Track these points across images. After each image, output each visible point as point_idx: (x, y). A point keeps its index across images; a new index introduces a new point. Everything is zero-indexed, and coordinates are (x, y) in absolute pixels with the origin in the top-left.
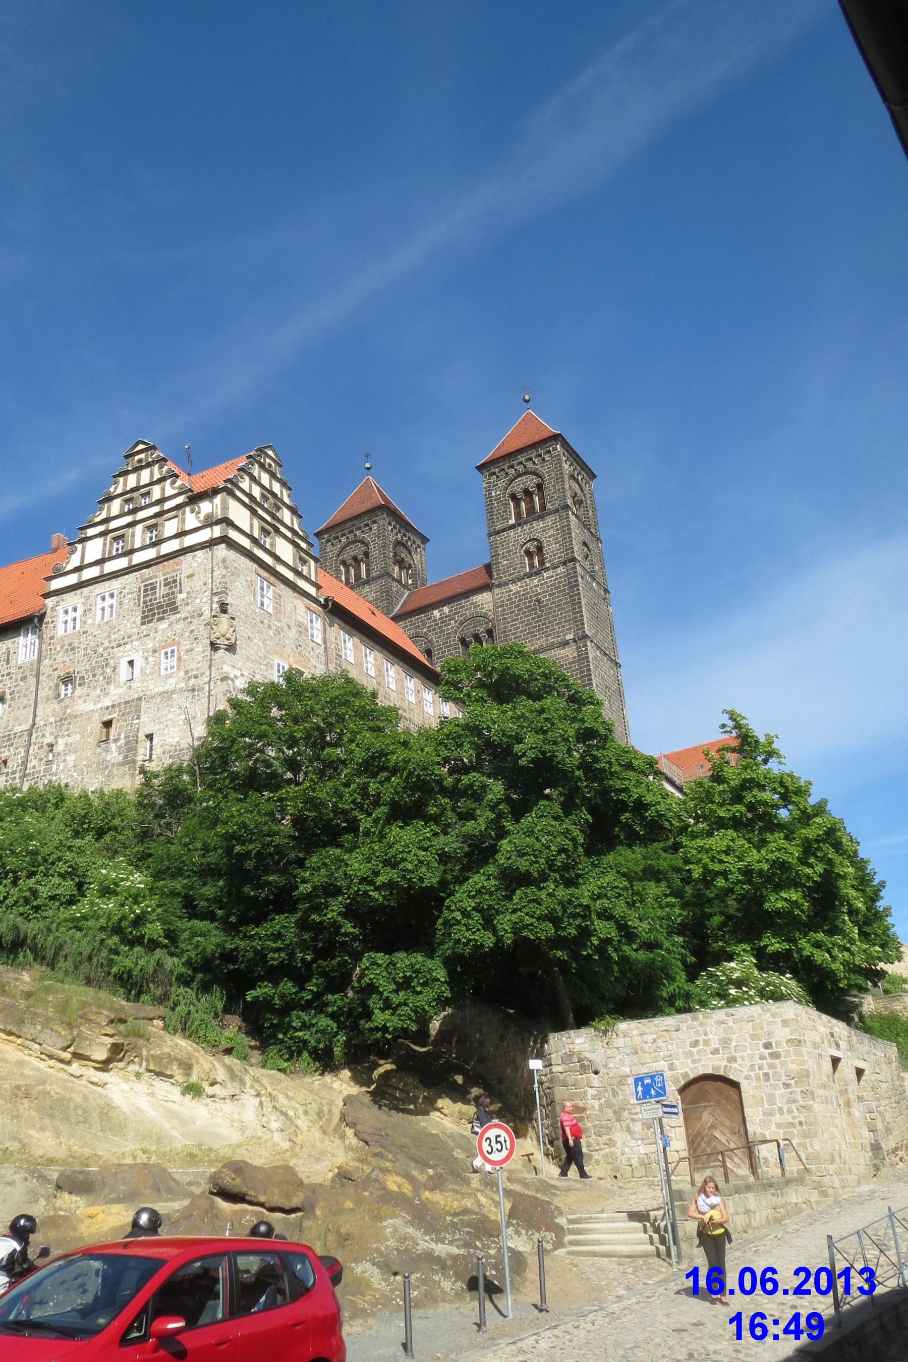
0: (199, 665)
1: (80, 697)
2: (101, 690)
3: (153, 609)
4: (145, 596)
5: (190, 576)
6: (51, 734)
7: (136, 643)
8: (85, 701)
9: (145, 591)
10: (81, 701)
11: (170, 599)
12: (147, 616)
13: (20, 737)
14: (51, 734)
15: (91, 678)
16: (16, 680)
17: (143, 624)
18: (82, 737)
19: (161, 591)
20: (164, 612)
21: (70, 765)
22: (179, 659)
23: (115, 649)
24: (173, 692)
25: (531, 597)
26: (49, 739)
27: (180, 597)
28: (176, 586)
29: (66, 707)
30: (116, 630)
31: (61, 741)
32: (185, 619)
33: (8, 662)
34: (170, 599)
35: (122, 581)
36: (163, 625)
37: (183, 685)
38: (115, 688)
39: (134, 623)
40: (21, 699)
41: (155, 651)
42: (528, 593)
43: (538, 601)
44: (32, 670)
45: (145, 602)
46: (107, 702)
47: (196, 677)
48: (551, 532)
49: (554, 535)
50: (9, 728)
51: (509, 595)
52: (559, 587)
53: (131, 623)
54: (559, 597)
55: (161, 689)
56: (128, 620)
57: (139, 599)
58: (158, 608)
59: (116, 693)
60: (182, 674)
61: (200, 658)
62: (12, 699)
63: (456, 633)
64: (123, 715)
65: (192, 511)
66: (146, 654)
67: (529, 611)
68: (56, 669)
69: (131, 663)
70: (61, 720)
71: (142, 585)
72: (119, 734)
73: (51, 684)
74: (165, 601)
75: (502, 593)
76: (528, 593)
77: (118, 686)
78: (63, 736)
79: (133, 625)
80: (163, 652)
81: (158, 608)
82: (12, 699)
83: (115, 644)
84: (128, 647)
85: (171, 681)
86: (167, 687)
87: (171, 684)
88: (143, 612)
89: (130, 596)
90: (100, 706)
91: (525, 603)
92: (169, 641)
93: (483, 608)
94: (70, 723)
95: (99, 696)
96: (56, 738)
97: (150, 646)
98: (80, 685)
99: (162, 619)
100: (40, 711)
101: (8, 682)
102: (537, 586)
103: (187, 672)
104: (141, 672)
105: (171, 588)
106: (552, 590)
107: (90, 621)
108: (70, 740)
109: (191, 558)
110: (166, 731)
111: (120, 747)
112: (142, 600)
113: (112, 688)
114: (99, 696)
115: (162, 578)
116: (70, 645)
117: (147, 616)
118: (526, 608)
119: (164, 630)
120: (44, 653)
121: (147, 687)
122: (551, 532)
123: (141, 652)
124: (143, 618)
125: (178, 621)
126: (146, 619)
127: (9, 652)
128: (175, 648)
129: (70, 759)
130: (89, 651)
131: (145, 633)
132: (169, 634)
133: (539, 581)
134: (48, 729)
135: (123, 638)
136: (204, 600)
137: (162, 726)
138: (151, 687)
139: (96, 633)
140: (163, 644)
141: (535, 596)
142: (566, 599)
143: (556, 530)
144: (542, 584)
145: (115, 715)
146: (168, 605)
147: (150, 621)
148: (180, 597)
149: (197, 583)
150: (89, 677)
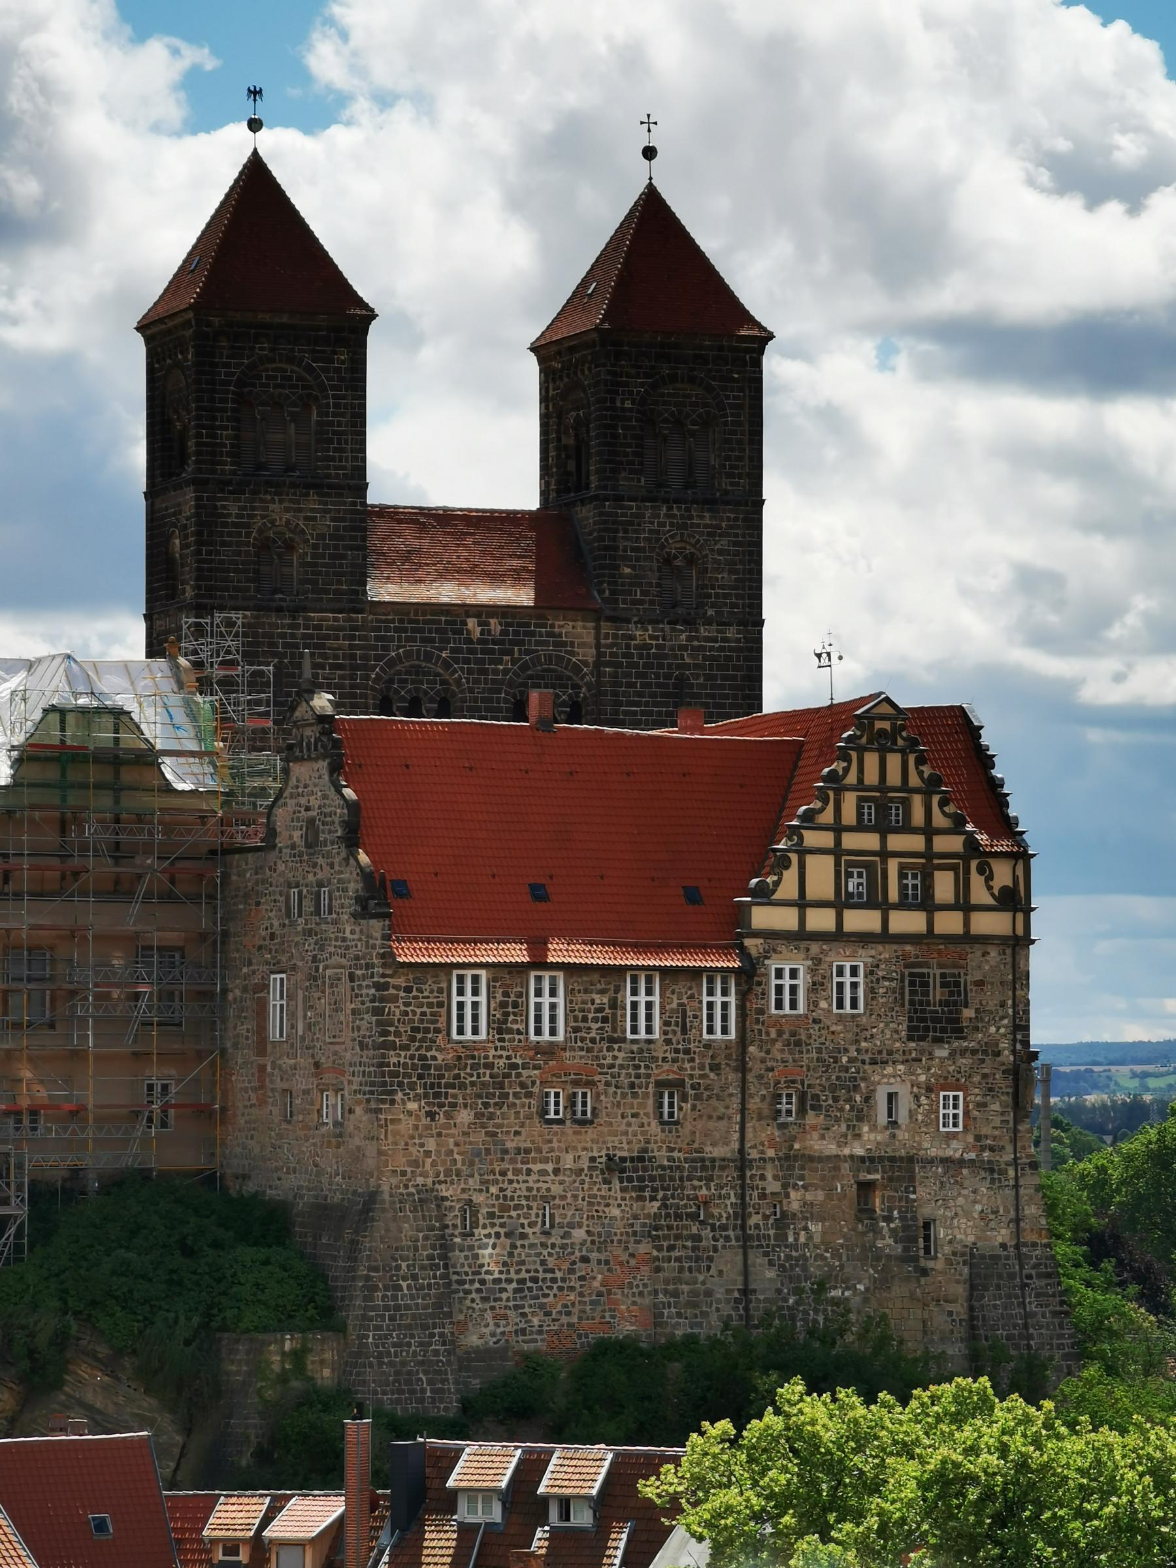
0: (996, 1133)
1: (814, 1128)
2: (848, 1126)
3: (924, 1020)
4: (912, 993)
5: (980, 984)
6: (776, 1178)
7: (901, 1067)
8: (823, 1137)
9: (912, 984)
10: (815, 1135)
11: (950, 1012)
12: (916, 1029)
13: (722, 1168)
14: (776, 1178)
15: (830, 1102)
16: (702, 1067)
17: (910, 1038)
18: (829, 1197)
19: (937, 994)
20: (943, 1030)
21: (817, 1239)
22: (966, 1113)
23: (867, 1067)
24: (961, 1163)
25: (670, 666)
26: (773, 1186)
27: (968, 1013)
28: (959, 995)
29: (793, 1139)
30: (868, 1034)
31: (793, 1194)
32: (974, 1052)
33: (684, 1031)
34: (950, 1012)
35: (873, 953)
36: (942, 1052)
37: (973, 1156)
38: (871, 1130)
39: (897, 1032)
40: (714, 1102)
41: (929, 1089)
42: (666, 656)
43: (681, 679)
44: (729, 1057)
45: (912, 1003)
46: (859, 1151)
47: (992, 1149)
48: (723, 544)
49: (728, 552)
50: (696, 1145)
51: (628, 647)
52: (726, 668)
53: (890, 1032)
54: (722, 687)
55: (941, 1154)
56: (887, 1025)
57: (902, 994)
58: (934, 1020)
59: (870, 1139)
60: (970, 1139)
61: (997, 1121)
62: (698, 1097)
63: (511, 684)
64: (890, 1179)
65: (981, 871)
66: (915, 1089)
67: (663, 695)
68: (772, 1069)
69: (891, 1097)
70: (787, 1158)
71: (907, 972)
72: (890, 1210)
73: (764, 1092)
74: (943, 1012)
75: (615, 636)
76: (666, 656)
77: (874, 1128)
78: (795, 1186)
79: (896, 1036)
80: (942, 1094)
81: (934, 1020)
82: (698, 1097)
83: (867, 1057)
84: (889, 1070)
85: (954, 1144)
86: (949, 1153)
87: (956, 1150)
88: (911, 1019)
89: (887, 983)
90: (847, 1151)
91: (657, 676)
92: (951, 1080)
93: (573, 654)
94: (802, 1168)
95: (845, 1136)
96: (785, 1186)
97: (923, 1078)
98: (813, 1108)
99: (938, 1041)
100: (749, 1134)
101: (687, 1065)
102: (683, 648)
103: (978, 1138)
104: (911, 1117)
105: (951, 994)
106: (711, 667)
107: (823, 1004)
108: (809, 1197)
109: (979, 953)
110: (955, 1221)
111: (893, 1232)
112: (907, 997)
113: (866, 1129)
114: (845, 1136)
115: (938, 972)
116: (793, 1034)
117: (916, 1029)
118: (659, 685)
119: (942, 1060)
120: (749, 1034)
121: (920, 1144)
122: (723, 544)
123: (909, 1085)
124: (910, 1029)
125: (963, 1052)
126: (916, 1032)
127: (684, 1012)
128: (961, 1094)
129: (815, 1228)
130: (825, 1056)
131: (914, 1055)
132: (951, 1069)
133: (689, 639)
134: (769, 1166)
135: (880, 1052)
136: (1002, 1030)
137: (948, 1214)
138: (926, 1145)
139: (833, 1028)
140: (941, 1081)
141: (679, 667)
142: (735, 697)
143: (735, 544)
144: (694, 648)
145: (878, 1176)
146: (949, 1021)
147: (922, 1039)
148: (968, 1013)
149: (991, 998)
150: (826, 1100)
